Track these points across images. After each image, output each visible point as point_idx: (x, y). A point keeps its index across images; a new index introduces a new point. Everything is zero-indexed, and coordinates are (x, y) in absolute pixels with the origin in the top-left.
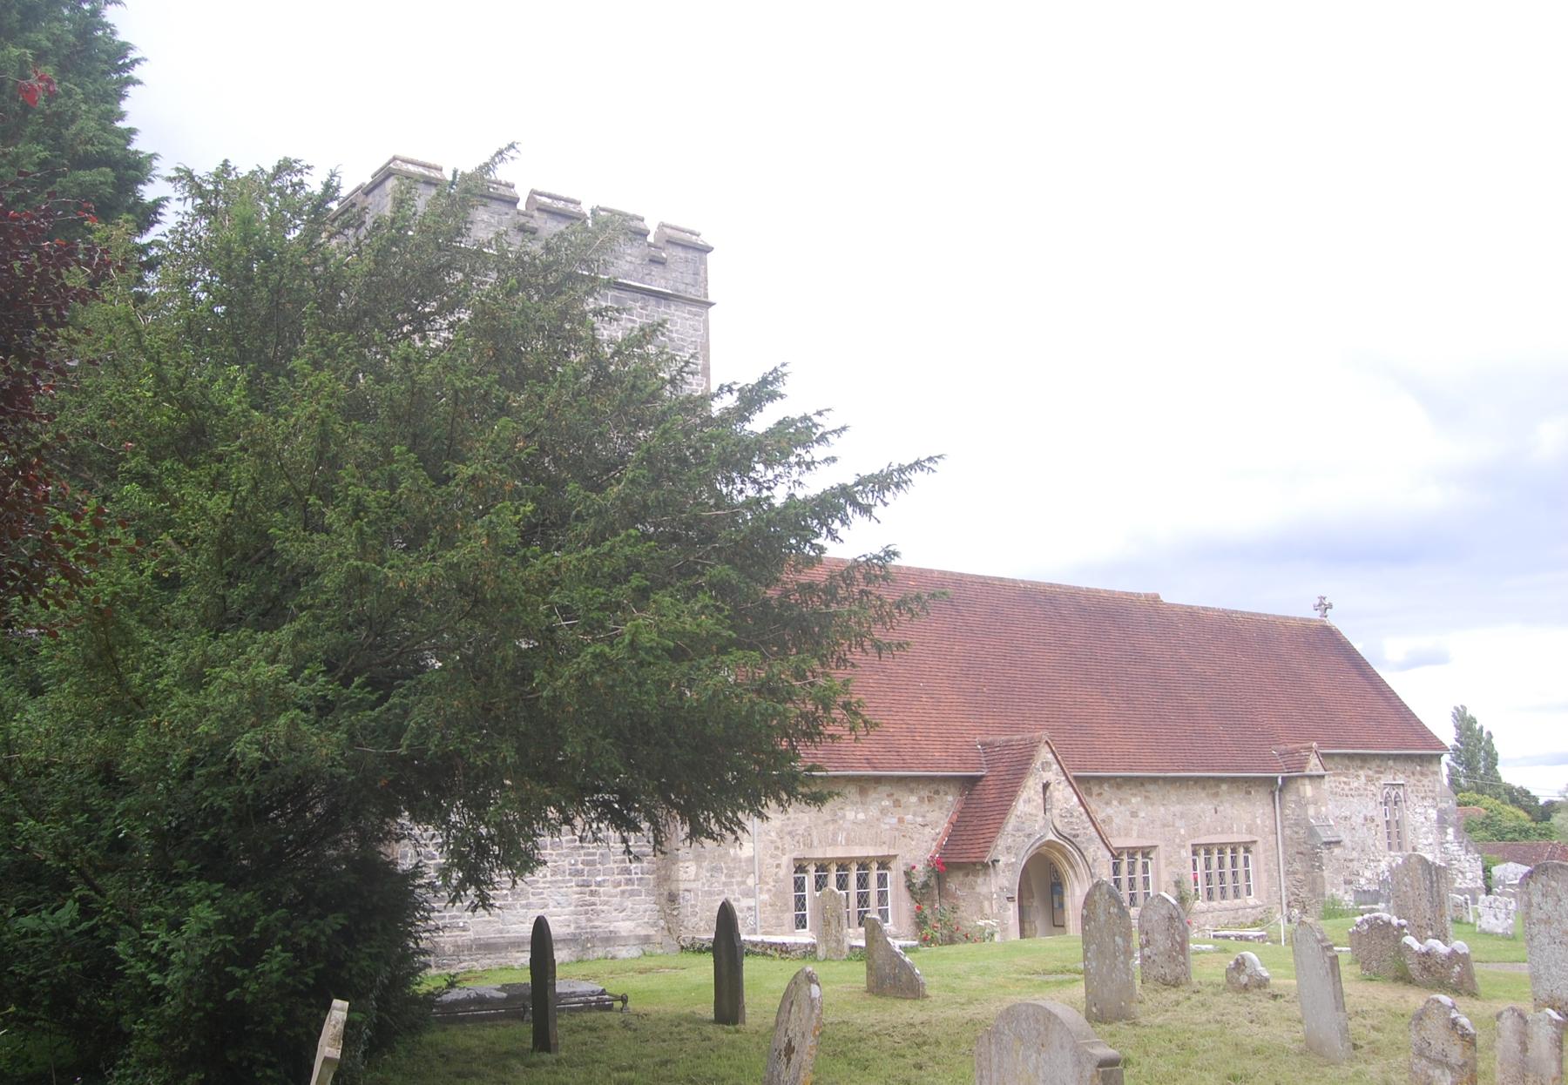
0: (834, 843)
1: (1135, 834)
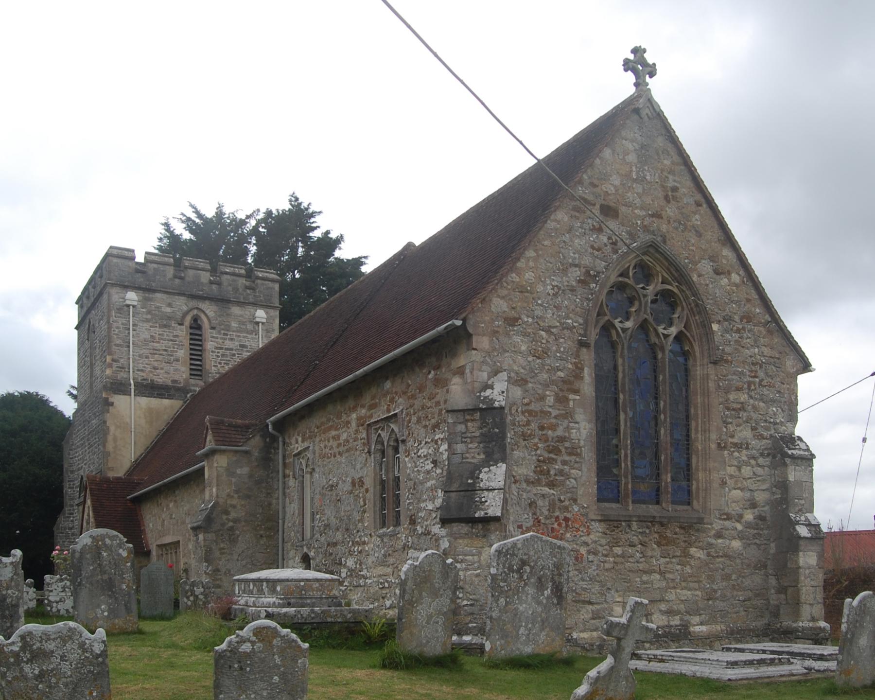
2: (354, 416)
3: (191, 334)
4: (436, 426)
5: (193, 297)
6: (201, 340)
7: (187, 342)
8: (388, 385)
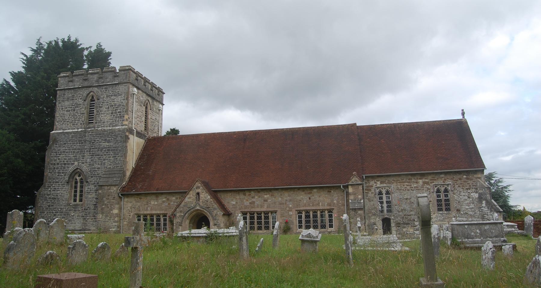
0: (147, 210)
1: (265, 207)
2: (421, 181)
4: (467, 189)
8: (442, 176)
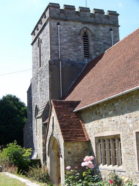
3: (84, 39)
5: (84, 23)
6: (88, 41)
7: (82, 42)
